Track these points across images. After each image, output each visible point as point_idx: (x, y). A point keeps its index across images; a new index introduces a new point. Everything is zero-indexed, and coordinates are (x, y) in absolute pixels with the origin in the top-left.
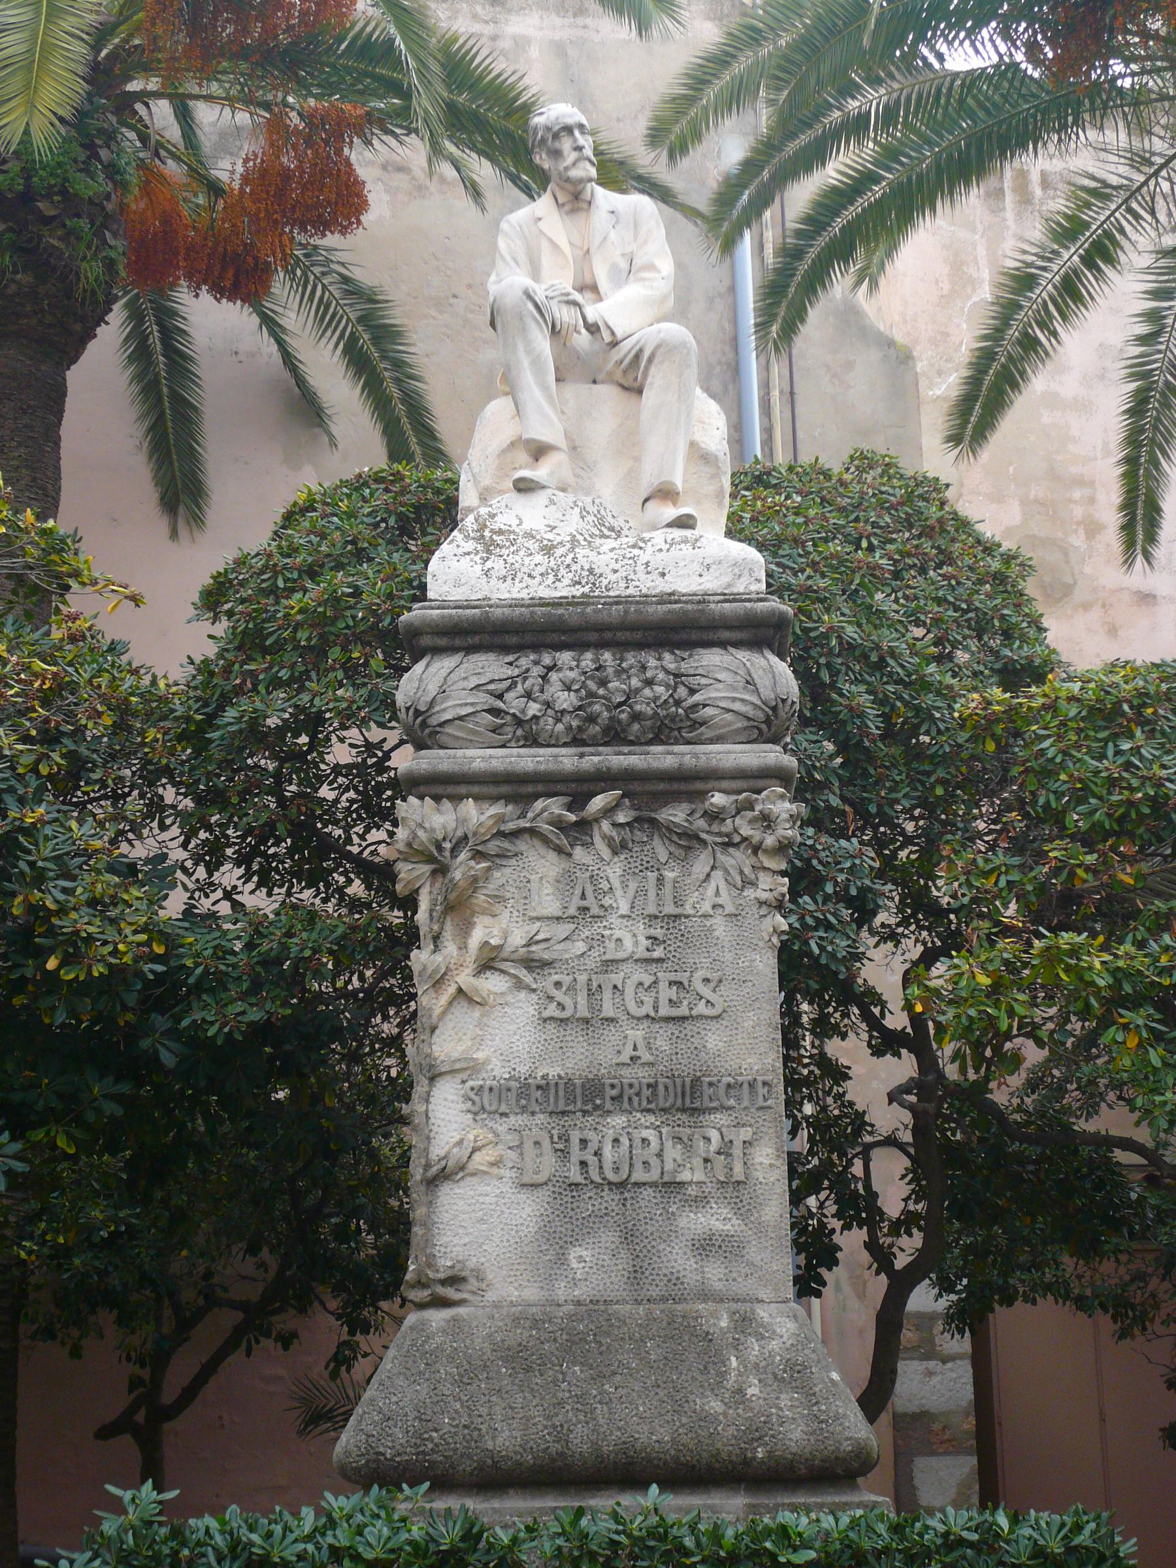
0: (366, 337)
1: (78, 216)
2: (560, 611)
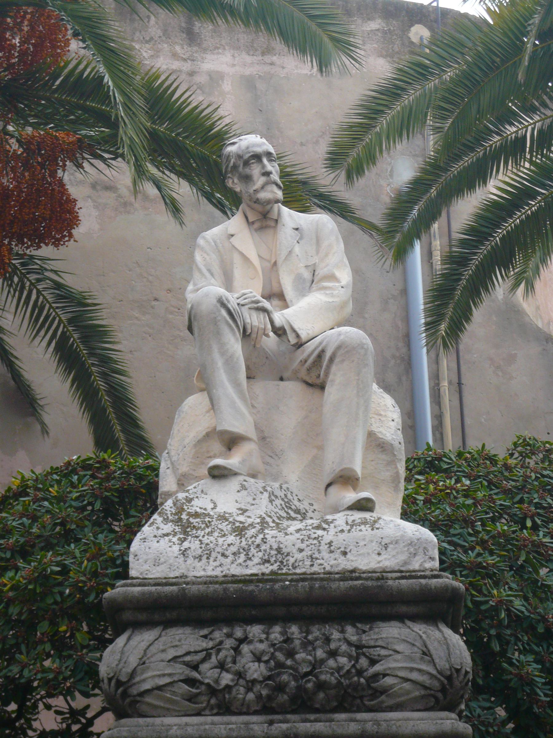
0: (76, 336)
2: (251, 587)
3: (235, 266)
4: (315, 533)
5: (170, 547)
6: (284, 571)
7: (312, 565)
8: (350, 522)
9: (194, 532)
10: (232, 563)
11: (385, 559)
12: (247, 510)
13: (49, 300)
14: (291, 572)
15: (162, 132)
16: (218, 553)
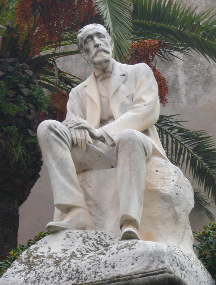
0: (200, 158)
1: (10, 125)
3: (87, 104)
4: (98, 257)
5: (20, 278)
6: (79, 283)
7: (95, 277)
8: (118, 248)
9: (34, 267)
10: (52, 282)
11: (136, 267)
12: (68, 249)
13: (179, 140)
14: (83, 283)
15: (172, 28)
16: (44, 277)
